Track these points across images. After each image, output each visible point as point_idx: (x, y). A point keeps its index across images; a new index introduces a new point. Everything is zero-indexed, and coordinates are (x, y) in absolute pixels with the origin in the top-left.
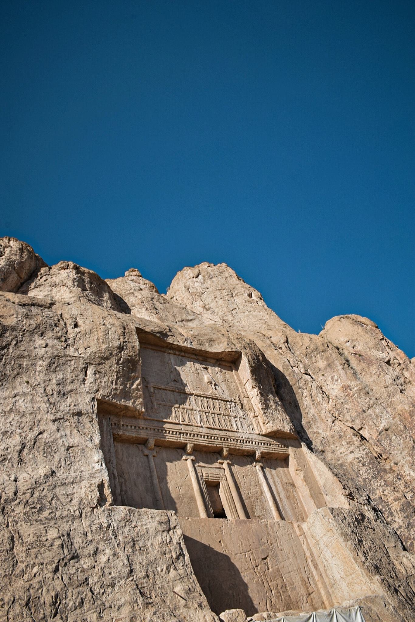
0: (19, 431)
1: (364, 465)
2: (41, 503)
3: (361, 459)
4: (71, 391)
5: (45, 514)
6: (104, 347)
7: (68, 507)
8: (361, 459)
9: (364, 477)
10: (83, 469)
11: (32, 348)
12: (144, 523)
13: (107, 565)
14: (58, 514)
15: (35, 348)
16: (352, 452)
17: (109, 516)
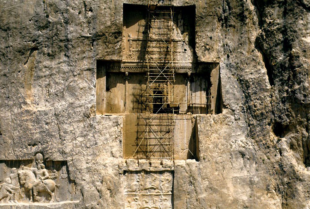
0: (62, 82)
1: (253, 84)
2: (69, 116)
3: (254, 80)
4: (84, 57)
5: (70, 120)
6: (102, 27)
7: (78, 117)
8: (254, 80)
9: (250, 91)
10: (86, 99)
11: (66, 34)
12: (107, 123)
13: (89, 140)
14: (75, 119)
15: (68, 34)
16: (251, 74)
17: (93, 121)
